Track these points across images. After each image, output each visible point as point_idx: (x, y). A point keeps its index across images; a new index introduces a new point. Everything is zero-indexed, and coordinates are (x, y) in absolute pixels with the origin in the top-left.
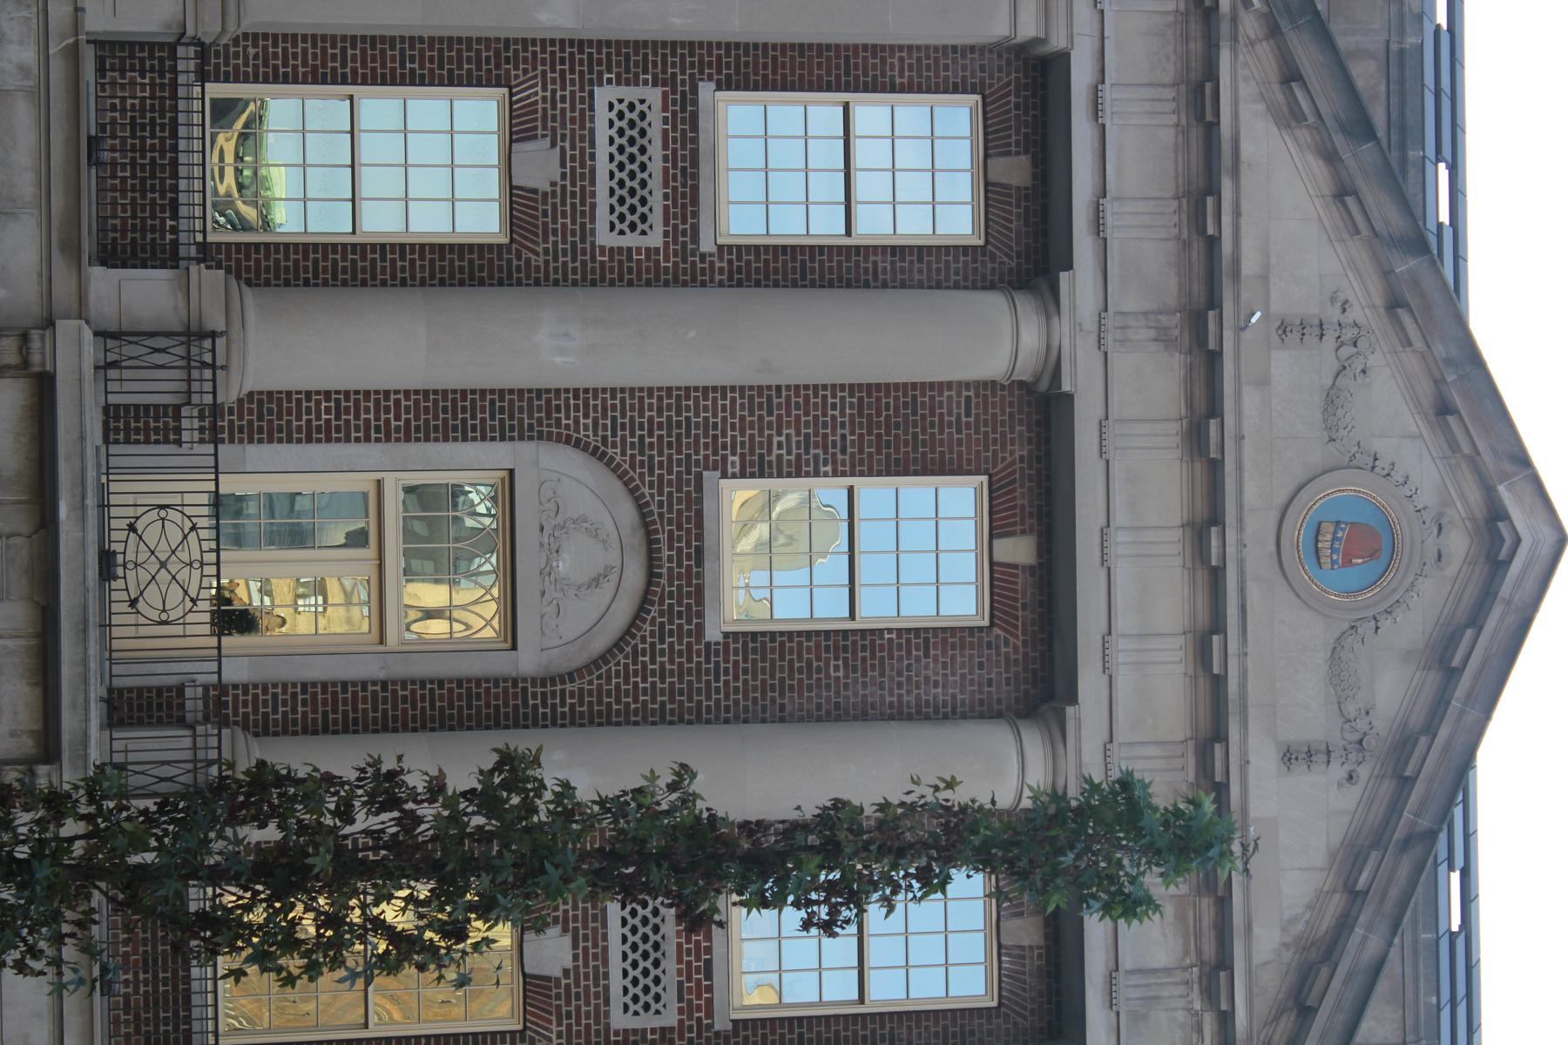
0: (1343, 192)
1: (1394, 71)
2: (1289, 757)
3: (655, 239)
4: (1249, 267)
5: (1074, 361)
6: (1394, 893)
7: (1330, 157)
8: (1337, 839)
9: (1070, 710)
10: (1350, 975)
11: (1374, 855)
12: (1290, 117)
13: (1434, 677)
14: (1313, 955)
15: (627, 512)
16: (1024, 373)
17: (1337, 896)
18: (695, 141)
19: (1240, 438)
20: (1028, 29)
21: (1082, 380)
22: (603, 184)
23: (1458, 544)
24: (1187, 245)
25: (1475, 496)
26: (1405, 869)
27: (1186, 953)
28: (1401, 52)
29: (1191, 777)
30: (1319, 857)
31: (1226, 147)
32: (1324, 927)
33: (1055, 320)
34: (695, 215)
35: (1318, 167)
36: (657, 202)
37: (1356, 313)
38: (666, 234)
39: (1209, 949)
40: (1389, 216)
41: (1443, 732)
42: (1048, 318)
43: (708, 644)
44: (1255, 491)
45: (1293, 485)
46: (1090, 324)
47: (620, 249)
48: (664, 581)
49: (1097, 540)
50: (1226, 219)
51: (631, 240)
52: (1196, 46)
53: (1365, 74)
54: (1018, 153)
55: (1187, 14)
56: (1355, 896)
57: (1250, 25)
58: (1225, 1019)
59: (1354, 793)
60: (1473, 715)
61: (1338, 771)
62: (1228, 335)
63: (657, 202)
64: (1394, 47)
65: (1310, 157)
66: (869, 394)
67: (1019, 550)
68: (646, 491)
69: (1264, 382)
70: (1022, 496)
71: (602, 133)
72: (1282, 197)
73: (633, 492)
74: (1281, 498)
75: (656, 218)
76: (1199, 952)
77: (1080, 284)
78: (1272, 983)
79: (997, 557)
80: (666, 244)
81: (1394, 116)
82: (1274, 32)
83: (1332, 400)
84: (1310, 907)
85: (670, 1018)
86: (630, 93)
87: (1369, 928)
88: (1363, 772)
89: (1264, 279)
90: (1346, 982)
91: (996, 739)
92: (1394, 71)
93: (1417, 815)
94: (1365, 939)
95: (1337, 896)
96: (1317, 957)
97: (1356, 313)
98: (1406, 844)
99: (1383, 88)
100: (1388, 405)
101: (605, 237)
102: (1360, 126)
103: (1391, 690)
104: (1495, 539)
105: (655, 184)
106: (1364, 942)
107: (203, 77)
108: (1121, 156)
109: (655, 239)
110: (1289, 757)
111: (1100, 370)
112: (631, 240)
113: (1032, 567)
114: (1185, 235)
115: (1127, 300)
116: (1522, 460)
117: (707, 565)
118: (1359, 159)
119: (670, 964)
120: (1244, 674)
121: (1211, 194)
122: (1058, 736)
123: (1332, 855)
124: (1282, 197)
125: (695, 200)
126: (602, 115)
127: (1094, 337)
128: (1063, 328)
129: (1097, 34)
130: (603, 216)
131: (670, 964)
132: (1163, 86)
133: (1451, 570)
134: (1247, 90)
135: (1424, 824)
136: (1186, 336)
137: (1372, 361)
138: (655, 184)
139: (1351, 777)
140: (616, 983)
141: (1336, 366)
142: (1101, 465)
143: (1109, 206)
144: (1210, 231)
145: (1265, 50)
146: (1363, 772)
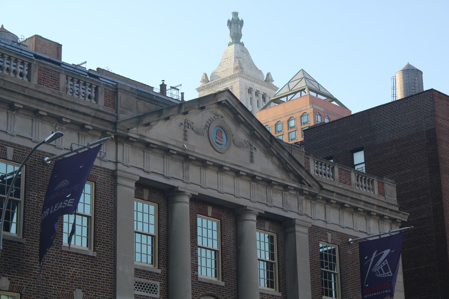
1: (141, 98)
3: (158, 283)
5: (193, 191)
6: (279, 147)
8: (263, 155)
9: (248, 208)
10: (290, 161)
11: (272, 149)
13: (242, 126)
14: (281, 166)
17: (273, 158)
18: (141, 270)
19: (211, 158)
20: (133, 185)
21: (197, 190)
26: (275, 143)
27: (280, 193)
28: (138, 95)
29: (255, 184)
31: (163, 145)
32: (278, 163)
33: (186, 193)
34: (154, 273)
36: (151, 282)
38: (157, 281)
40: (176, 109)
41: (255, 128)
42: (185, 195)
43: (225, 285)
44: (208, 153)
45: (210, 146)
47: (160, 293)
48: (215, 293)
49: (219, 194)
50: (175, 149)
54: (143, 192)
55: (132, 145)
61: (254, 151)
62: (195, 155)
63: (151, 282)
64: (136, 96)
65: (159, 124)
67: (210, 210)
68: (200, 294)
69: (194, 147)
72: (163, 132)
74: (212, 149)
76: (281, 190)
79: (147, 199)
80: (159, 281)
81: (148, 100)
84: (273, 164)
87: (283, 154)
90: (291, 162)
92: (141, 98)
93: (267, 138)
94: (285, 156)
95: (273, 158)
96: (284, 167)
97: (183, 122)
98: (271, 142)
99: (143, 101)
100: (198, 119)
101: (158, 296)
103: (241, 135)
106: (285, 156)
108: (158, 169)
109: (158, 283)
110: (252, 161)
111: (193, 185)
112: (158, 290)
113: (213, 208)
114: (170, 158)
117: (213, 283)
120: (247, 169)
121: (255, 177)
122: (250, 212)
123: (266, 157)
124: (163, 132)
125: (151, 272)
127: (187, 185)
129: (136, 169)
130: (154, 295)
132: (144, 155)
135: (269, 137)
136: (188, 163)
139: (255, 149)
141: (191, 130)
142: (208, 189)
144: (176, 153)
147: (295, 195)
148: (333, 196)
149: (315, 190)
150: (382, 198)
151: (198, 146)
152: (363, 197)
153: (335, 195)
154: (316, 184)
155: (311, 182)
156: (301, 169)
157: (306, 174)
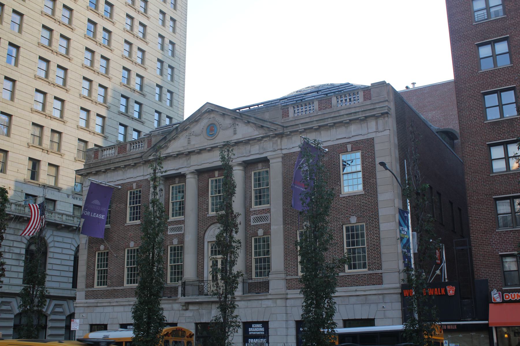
0: (174, 139)
2: (235, 134)
7: (170, 141)
12: (167, 147)
15: (212, 226)
21: (193, 169)
22: (263, 223)
23: (212, 116)
24: (180, 158)
25: (206, 115)
35: (172, 142)
56: (249, 122)
58: (263, 137)
59: (239, 124)
60: (227, 111)
63: (179, 226)
66: (199, 196)
71: (173, 233)
77: (182, 171)
83: (196, 136)
86: (252, 220)
88: (237, 123)
102: (165, 138)
105: (177, 226)
107: (252, 279)
115: (185, 164)
116: (199, 110)
118: (169, 138)
126: (255, 224)
128: (187, 172)
133: (215, 116)
137: (192, 131)
138: (177, 226)
140: (265, 222)
143: (175, 168)
147: (270, 140)
148: (299, 127)
149: (280, 131)
150: (368, 102)
151: (197, 143)
152: (342, 111)
153: (300, 125)
154: (279, 127)
155: (273, 127)
156: (265, 123)
157: (270, 124)
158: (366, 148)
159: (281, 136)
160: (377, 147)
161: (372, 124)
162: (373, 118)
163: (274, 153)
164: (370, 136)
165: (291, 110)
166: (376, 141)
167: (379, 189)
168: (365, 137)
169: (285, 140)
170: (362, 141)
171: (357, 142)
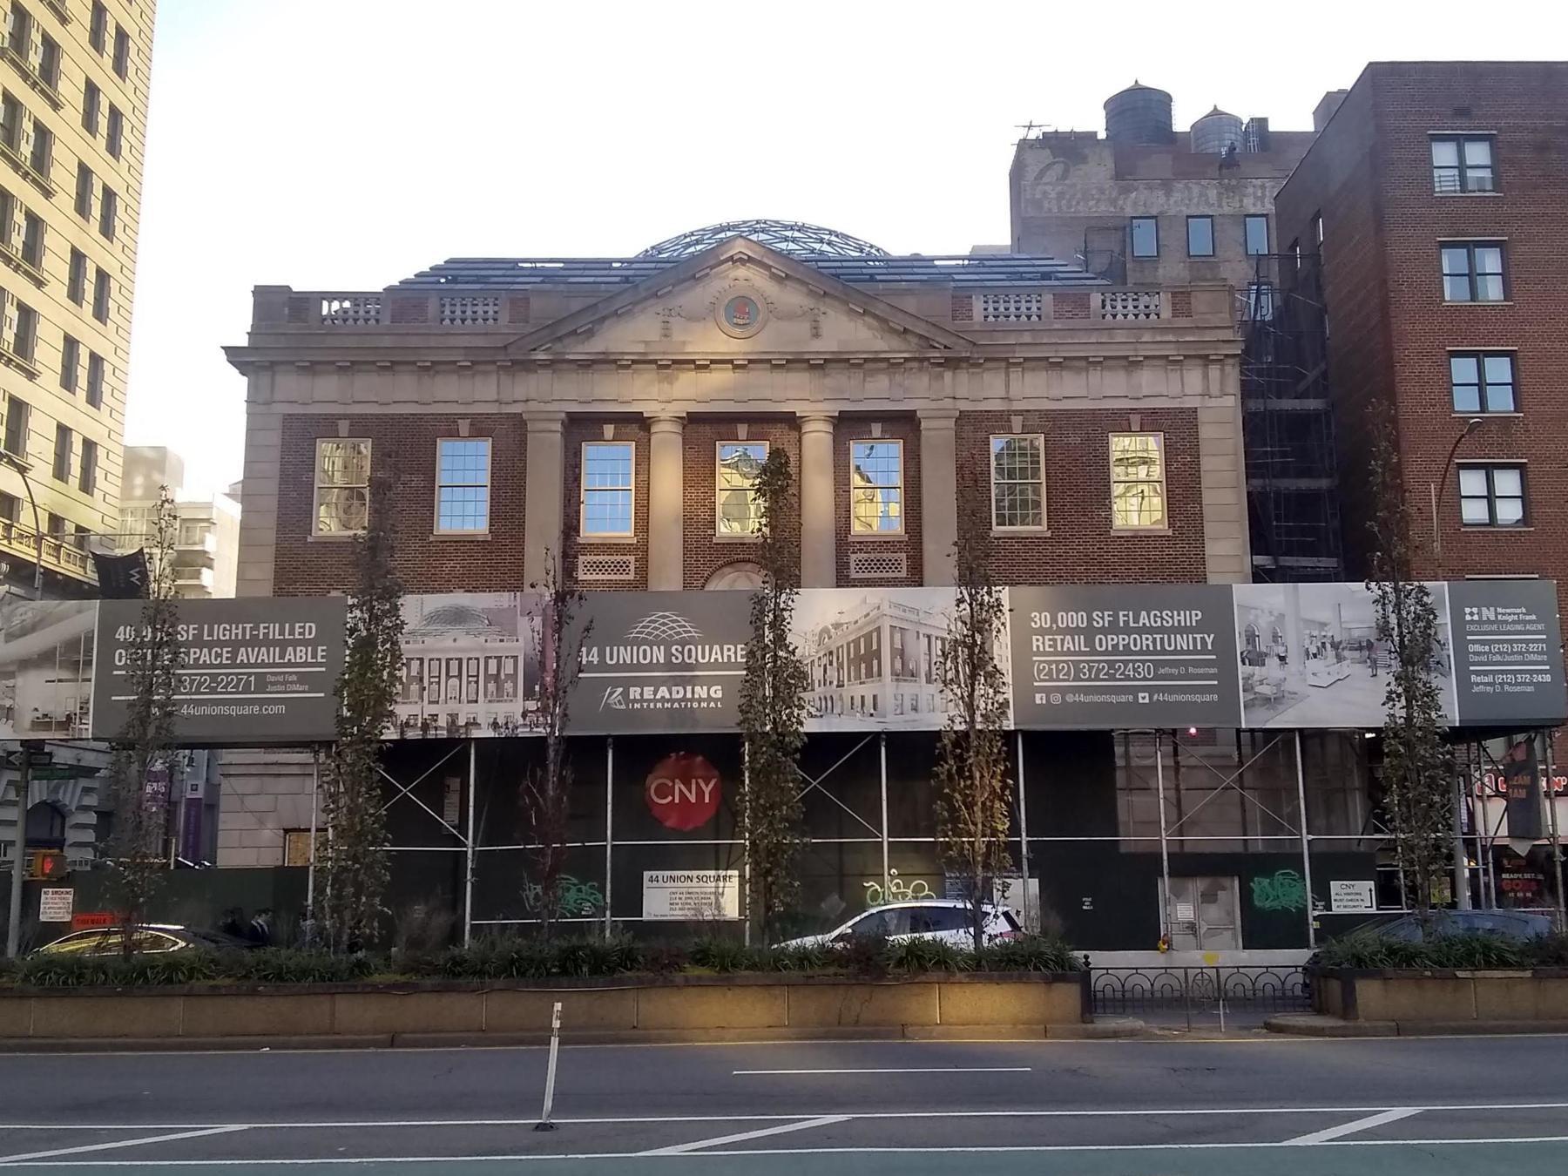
2: (817, 335)
4: (641, 348)
7: (603, 319)
12: (590, 333)
16: (678, 429)
20: (558, 427)
21: (682, 409)
24: (635, 371)
30: (852, 324)
37: (660, 310)
39: (884, 365)
46: (663, 406)
51: (632, 567)
52: (565, 366)
53: (576, 305)
57: (558, 347)
58: (906, 359)
70: (723, 428)
73: (720, 567)
75: (625, 558)
78: (896, 343)
82: (560, 339)
85: (904, 555)
89: (646, 343)
91: (808, 440)
101: (631, 577)
104: (740, 259)
119: (885, 556)
128: (663, 415)
131: (885, 556)
134: (580, 349)
138: (613, 558)
145: (566, 341)
146: (823, 309)
147: (920, 369)
158: (1177, 429)
159: (953, 363)
160: (1205, 432)
161: (1193, 378)
162: (1199, 362)
163: (934, 405)
164: (1189, 403)
165: (978, 306)
166: (1202, 416)
167: (1209, 529)
168: (1175, 404)
169: (963, 376)
170: (1167, 412)
171: (1154, 411)
